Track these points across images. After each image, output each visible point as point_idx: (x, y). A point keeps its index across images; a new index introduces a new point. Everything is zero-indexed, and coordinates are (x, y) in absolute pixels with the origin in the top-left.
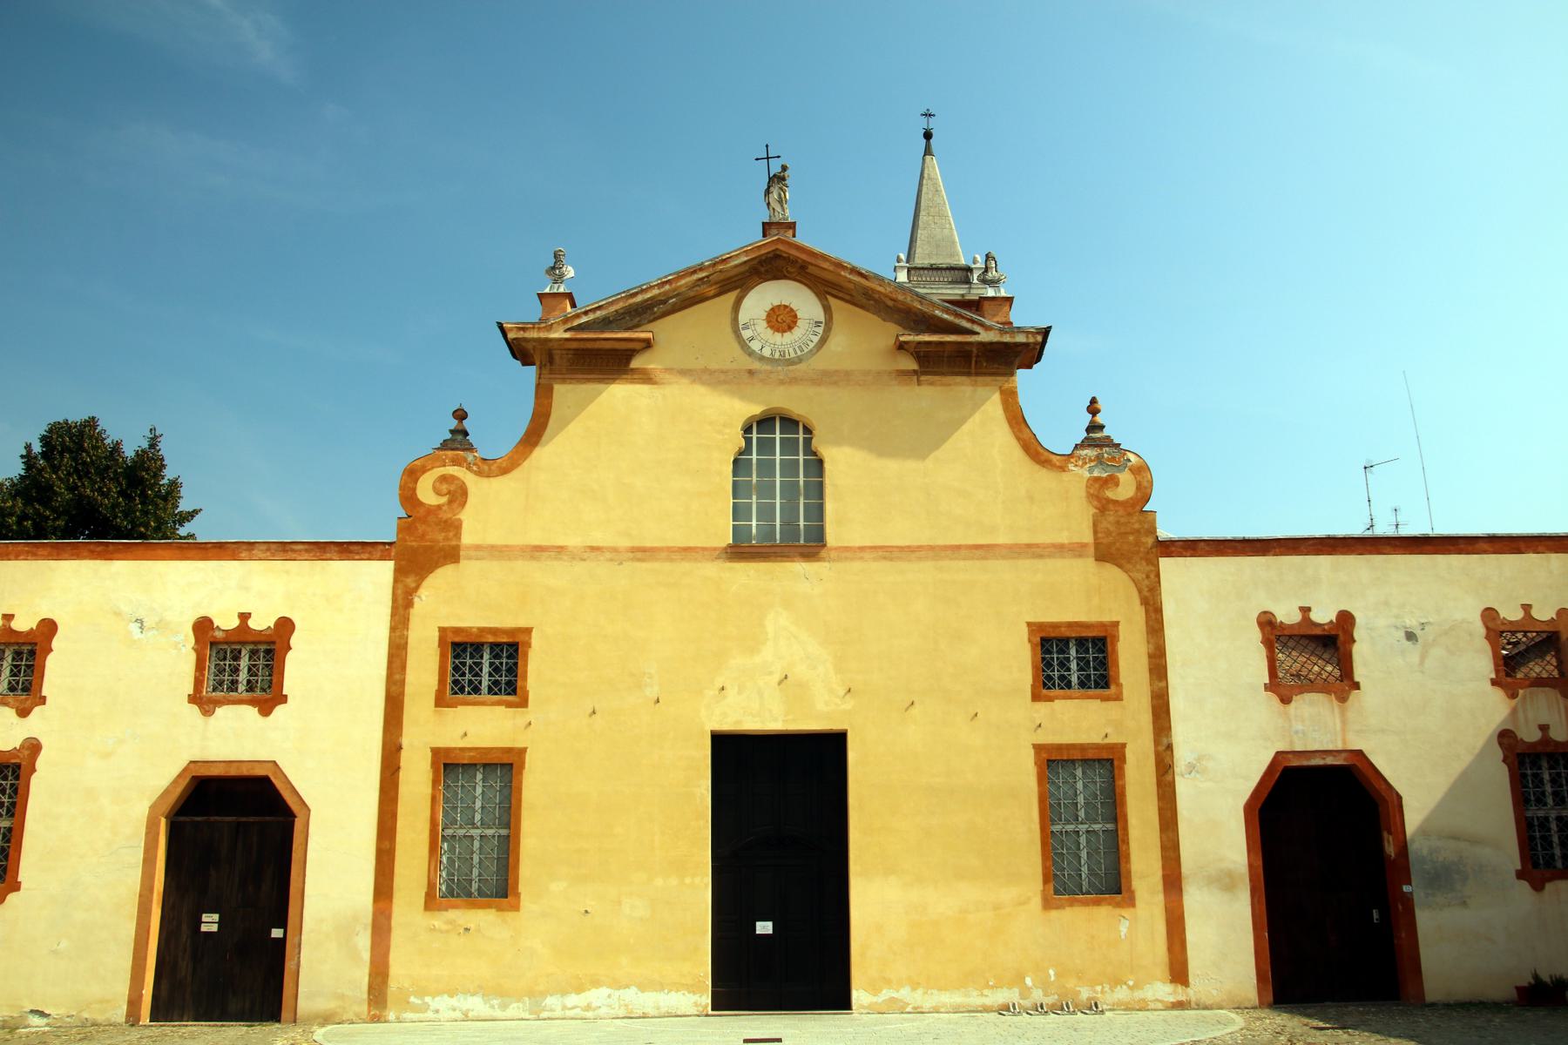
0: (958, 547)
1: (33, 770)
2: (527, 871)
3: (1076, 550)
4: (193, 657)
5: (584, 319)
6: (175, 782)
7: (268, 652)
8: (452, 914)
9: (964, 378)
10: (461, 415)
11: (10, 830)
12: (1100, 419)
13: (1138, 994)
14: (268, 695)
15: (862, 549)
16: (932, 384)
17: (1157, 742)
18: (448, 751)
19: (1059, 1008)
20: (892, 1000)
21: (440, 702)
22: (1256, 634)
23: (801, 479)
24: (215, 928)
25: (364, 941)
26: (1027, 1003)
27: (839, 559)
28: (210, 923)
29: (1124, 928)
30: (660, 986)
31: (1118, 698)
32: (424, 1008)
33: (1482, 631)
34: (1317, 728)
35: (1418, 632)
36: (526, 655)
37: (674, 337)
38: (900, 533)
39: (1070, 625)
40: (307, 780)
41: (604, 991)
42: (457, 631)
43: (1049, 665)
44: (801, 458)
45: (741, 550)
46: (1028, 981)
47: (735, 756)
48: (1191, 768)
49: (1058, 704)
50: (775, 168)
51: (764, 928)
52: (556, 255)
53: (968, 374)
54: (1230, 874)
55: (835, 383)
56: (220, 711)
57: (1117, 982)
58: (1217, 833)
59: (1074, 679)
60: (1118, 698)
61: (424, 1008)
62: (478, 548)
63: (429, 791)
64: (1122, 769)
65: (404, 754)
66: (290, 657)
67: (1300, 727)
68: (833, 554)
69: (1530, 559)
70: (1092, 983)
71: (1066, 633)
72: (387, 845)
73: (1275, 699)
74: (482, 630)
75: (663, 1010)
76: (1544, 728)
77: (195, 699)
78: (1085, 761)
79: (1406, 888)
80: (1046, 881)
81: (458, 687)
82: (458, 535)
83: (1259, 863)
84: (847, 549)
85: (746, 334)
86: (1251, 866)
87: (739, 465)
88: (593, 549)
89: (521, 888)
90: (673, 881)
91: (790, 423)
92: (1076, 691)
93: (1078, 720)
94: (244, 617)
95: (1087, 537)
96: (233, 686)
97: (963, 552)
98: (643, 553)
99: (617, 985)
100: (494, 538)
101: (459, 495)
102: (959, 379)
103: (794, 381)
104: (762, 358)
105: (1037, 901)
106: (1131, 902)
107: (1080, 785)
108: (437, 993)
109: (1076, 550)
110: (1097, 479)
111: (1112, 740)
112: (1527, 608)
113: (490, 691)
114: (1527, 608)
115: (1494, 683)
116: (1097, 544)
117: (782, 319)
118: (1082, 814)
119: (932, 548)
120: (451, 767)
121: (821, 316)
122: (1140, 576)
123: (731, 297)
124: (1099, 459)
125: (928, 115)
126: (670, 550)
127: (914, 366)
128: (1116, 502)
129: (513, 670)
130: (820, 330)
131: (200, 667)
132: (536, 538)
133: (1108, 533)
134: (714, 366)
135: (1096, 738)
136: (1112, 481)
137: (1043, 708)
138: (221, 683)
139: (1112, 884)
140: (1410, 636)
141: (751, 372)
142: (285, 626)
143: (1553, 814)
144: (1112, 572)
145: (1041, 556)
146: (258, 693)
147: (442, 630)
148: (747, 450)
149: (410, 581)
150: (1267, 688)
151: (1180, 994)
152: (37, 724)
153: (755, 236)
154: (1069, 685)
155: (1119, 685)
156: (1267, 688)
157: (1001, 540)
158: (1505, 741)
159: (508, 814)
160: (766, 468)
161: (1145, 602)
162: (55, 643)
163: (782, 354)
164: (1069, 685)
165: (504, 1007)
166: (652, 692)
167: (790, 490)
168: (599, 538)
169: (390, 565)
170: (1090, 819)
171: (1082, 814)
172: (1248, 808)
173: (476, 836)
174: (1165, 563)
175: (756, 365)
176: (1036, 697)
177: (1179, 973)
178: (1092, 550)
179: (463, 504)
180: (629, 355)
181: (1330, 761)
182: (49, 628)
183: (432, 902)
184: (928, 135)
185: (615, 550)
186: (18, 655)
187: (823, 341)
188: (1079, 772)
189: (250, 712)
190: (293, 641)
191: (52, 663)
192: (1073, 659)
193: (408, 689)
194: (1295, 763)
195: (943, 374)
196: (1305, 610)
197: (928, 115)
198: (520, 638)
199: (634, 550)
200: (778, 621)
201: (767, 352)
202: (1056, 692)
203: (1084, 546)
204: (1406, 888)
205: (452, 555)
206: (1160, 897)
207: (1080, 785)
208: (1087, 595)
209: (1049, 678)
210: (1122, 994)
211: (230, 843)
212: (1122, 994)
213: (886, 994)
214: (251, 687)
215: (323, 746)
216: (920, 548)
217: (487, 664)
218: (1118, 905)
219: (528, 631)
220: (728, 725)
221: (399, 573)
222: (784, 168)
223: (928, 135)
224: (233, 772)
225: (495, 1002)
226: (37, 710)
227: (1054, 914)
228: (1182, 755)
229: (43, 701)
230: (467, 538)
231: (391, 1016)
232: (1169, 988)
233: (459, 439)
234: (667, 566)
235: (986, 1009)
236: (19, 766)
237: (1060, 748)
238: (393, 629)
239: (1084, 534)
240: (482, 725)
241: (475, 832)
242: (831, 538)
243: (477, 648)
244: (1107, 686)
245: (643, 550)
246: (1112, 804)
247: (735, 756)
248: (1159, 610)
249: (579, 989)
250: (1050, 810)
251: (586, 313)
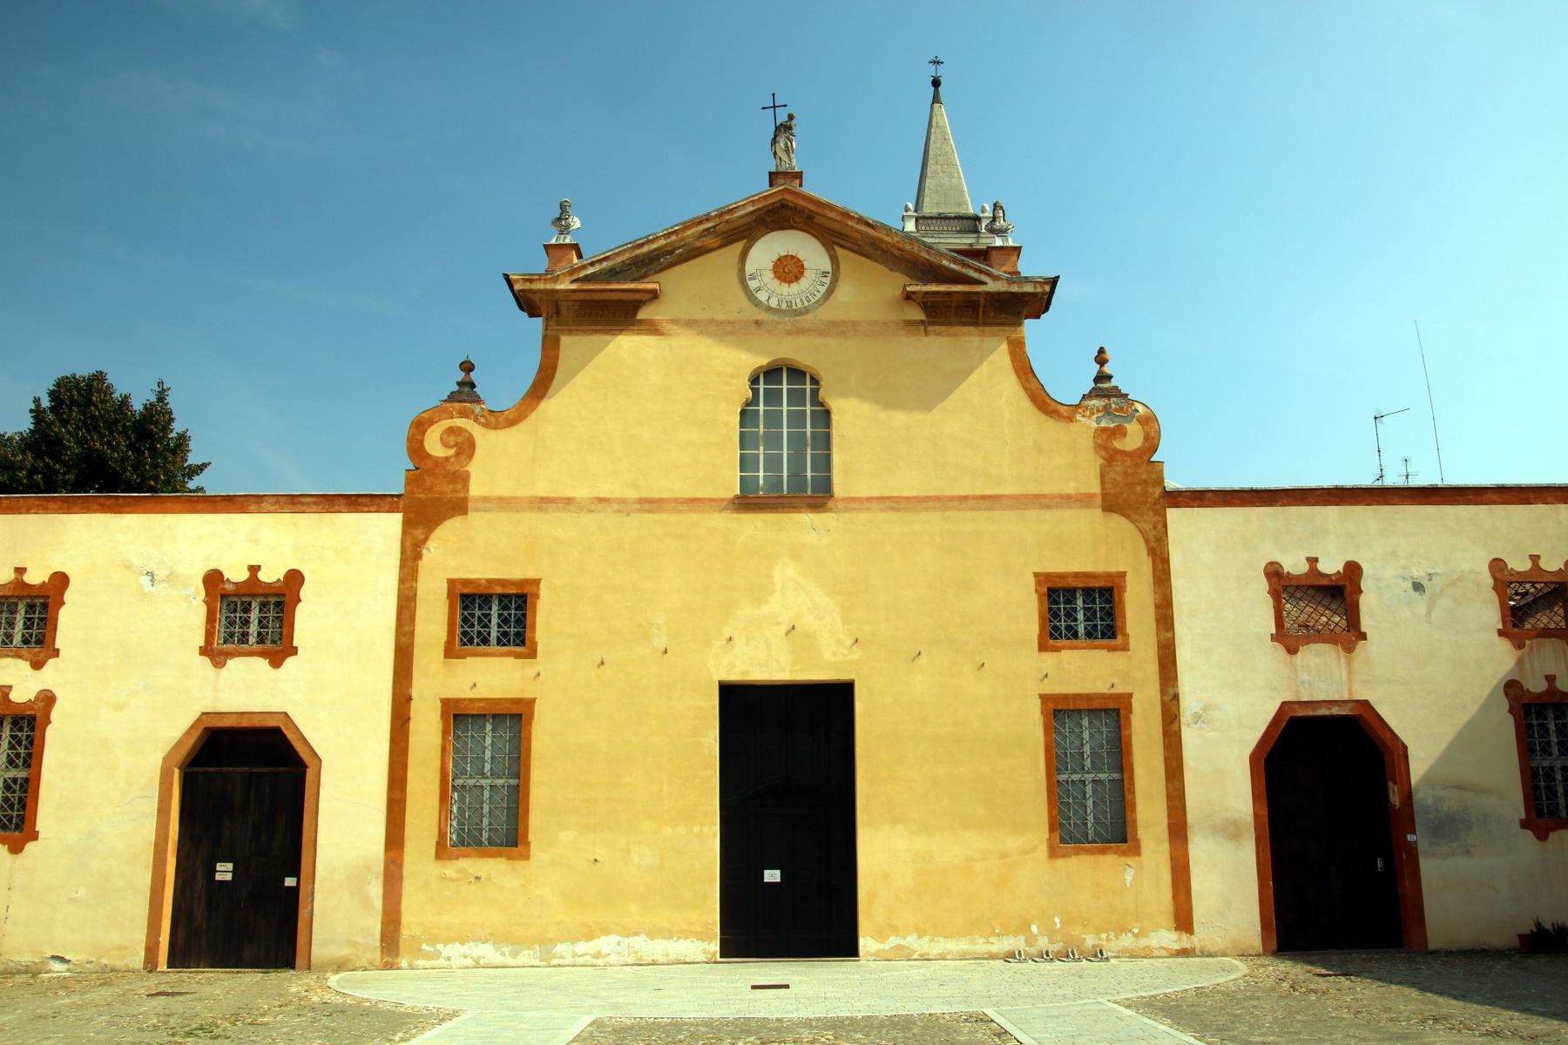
0: (966, 498)
1: (48, 722)
2: (537, 819)
3: (1083, 500)
4: (203, 609)
5: (590, 270)
6: (188, 733)
7: (278, 604)
8: (464, 863)
9: (971, 329)
10: (467, 367)
11: (27, 780)
12: (1107, 369)
13: (1143, 942)
14: (278, 647)
15: (869, 499)
16: (939, 334)
17: (1163, 692)
18: (457, 701)
19: (1064, 956)
20: (899, 947)
21: (449, 653)
22: (1263, 585)
23: (809, 430)
24: (229, 877)
25: (376, 890)
26: (1033, 950)
27: (846, 510)
28: (224, 872)
29: (1129, 876)
30: (669, 934)
31: (1125, 648)
32: (437, 955)
33: (1490, 582)
34: (1323, 678)
35: (1425, 583)
36: (534, 607)
37: (680, 289)
38: (908, 483)
39: (1077, 575)
41: (613, 939)
42: (466, 582)
43: (1056, 615)
44: (808, 408)
45: (748, 501)
46: (1034, 929)
47: (743, 706)
48: (1197, 718)
49: (1064, 654)
50: (782, 117)
51: (772, 876)
52: (562, 206)
53: (976, 324)
54: (1235, 823)
55: (843, 334)
56: (231, 663)
57: (1122, 929)
58: (1223, 782)
59: (1081, 629)
60: (1125, 648)
61: (437, 955)
62: (486, 499)
63: (438, 741)
64: (1128, 719)
65: (414, 704)
66: (299, 608)
67: (1306, 677)
68: (840, 505)
69: (1540, 509)
70: (1098, 931)
71: (1072, 583)
72: (397, 794)
73: (1281, 650)
74: (490, 581)
75: (672, 957)
76: (1550, 679)
77: (205, 651)
78: (1091, 711)
79: (1410, 838)
80: (1052, 829)
81: (467, 639)
82: (466, 487)
83: (1264, 812)
84: (853, 500)
85: (753, 285)
86: (1256, 815)
87: (746, 416)
88: (601, 500)
89: (531, 837)
90: (682, 830)
91: (797, 374)
92: (1082, 641)
93: (1085, 670)
94: (254, 570)
95: (1094, 487)
96: (244, 637)
97: (971, 503)
98: (650, 504)
99: (627, 932)
100: (503, 489)
101: (466, 447)
102: (966, 329)
103: (801, 331)
104: (769, 309)
105: (1042, 849)
106: (1136, 850)
107: (1086, 735)
108: (451, 940)
109: (1083, 500)
110: (1104, 430)
111: (1119, 689)
112: (1535, 559)
113: (499, 642)
114: (1535, 559)
115: (1501, 633)
116: (1104, 495)
117: (789, 269)
118: (1088, 763)
119: (938, 498)
120: (461, 718)
121: (829, 268)
122: (1147, 526)
123: (737, 247)
124: (1106, 409)
125: (937, 62)
126: (677, 501)
127: (920, 315)
128: (1123, 453)
129: (521, 621)
130: (827, 280)
131: (210, 618)
132: (543, 490)
133: (1115, 484)
134: (720, 317)
135: (1101, 688)
136: (1119, 431)
137: (1049, 657)
138: (232, 635)
139: (1118, 833)
140: (1418, 587)
141: (758, 323)
142: (295, 579)
143: (1558, 764)
144: (1119, 523)
145: (1048, 507)
146: (269, 645)
147: (451, 582)
148: (754, 401)
149: (419, 533)
150: (1273, 638)
151: (1185, 941)
152: (51, 676)
153: (761, 186)
154: (1076, 636)
155: (1126, 636)
156: (1273, 638)
157: (1007, 491)
158: (1511, 691)
159: (517, 764)
160: (773, 419)
161: (1152, 552)
162: (67, 596)
163: (789, 304)
164: (1076, 636)
165: (515, 954)
166: (660, 643)
167: (797, 441)
168: (605, 489)
169: (397, 518)
170: (1096, 768)
171: (1088, 763)
172: (1254, 758)
173: (486, 787)
174: (1172, 513)
175: (763, 316)
176: (1043, 647)
177: (1184, 921)
178: (1099, 500)
179: (471, 456)
180: (635, 306)
181: (1336, 711)
182: (60, 581)
183: (442, 851)
184: (936, 83)
185: (623, 501)
186: (31, 608)
187: (830, 291)
188: (1085, 722)
189: (261, 664)
190: (304, 593)
191: (64, 615)
193: (418, 641)
194: (1301, 713)
195: (950, 324)
196: (1313, 561)
197: (937, 62)
198: (528, 590)
199: (641, 501)
200: (785, 572)
201: (773, 303)
202: (1064, 642)
203: (1091, 496)
204: (1410, 838)
205: (460, 507)
206: (1166, 846)
207: (1086, 735)
208: (1094, 545)
209: (1056, 628)
210: (1127, 941)
211: (242, 792)
212: (1127, 941)
213: (893, 941)
214: (261, 639)
215: (334, 697)
216: (927, 499)
217: (496, 615)
218: (1124, 854)
219: (537, 582)
220: (735, 676)
221: (408, 525)
222: (791, 117)
223: (936, 83)
224: (245, 723)
225: (506, 949)
226: (51, 662)
227: (1060, 862)
228: (1189, 705)
229: (56, 653)
230: (477, 488)
231: (404, 963)
232: (1174, 935)
233: (466, 392)
234: (675, 517)
235: (992, 957)
236: (34, 718)
237: (1066, 697)
238: (402, 581)
239: (1092, 484)
240: (490, 676)
241: (485, 782)
242: (839, 489)
243: (486, 599)
244: (1113, 636)
245: (651, 501)
246: (1119, 755)
247: (743, 706)
248: (1166, 561)
249: (589, 937)
250: (1056, 760)
251: (592, 264)
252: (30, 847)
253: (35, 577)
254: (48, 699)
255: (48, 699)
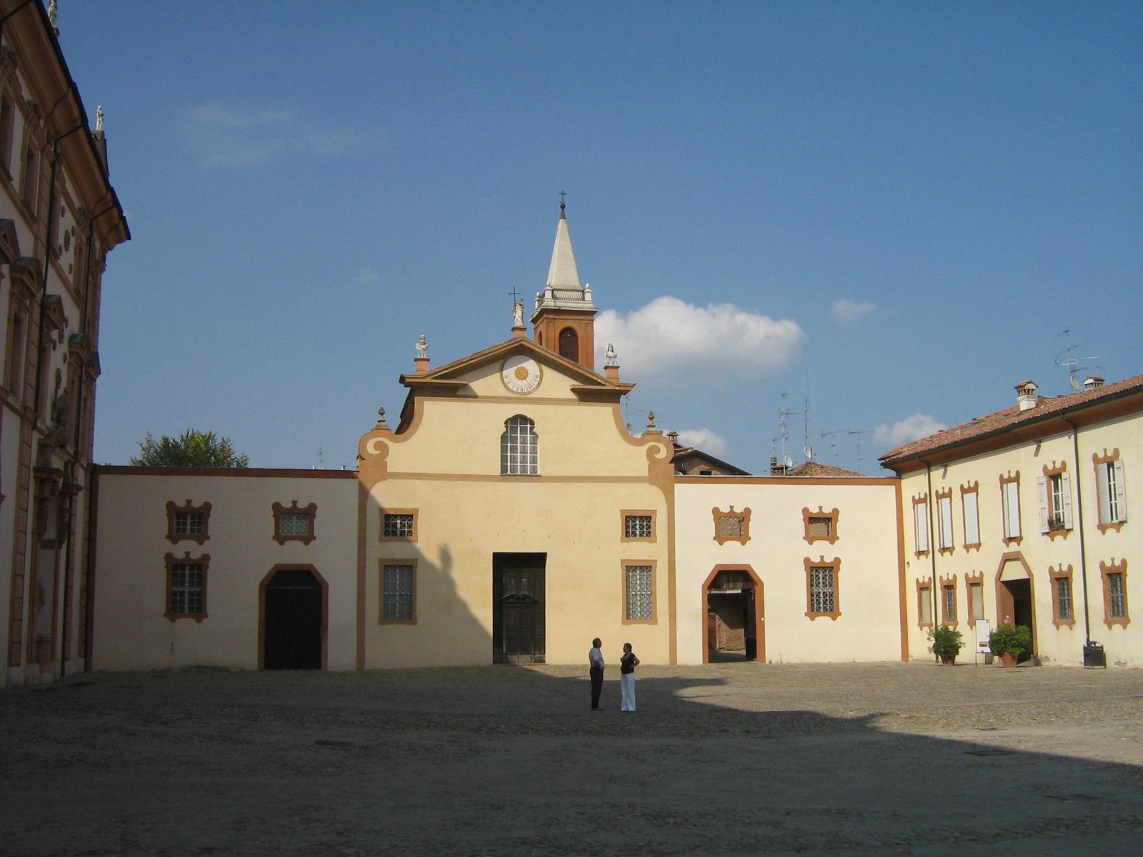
34: (733, 554)
40: (326, 571)
85: (506, 380)
91: (524, 419)
130: (538, 379)
141: (508, 398)
152: (207, 548)
187: (539, 384)
192: (637, 525)
201: (515, 389)
208: (646, 498)
219: (416, 510)
230: (389, 470)
236: (201, 565)
252: (205, 620)
253: (197, 504)
254: (206, 558)
255: (206, 558)
